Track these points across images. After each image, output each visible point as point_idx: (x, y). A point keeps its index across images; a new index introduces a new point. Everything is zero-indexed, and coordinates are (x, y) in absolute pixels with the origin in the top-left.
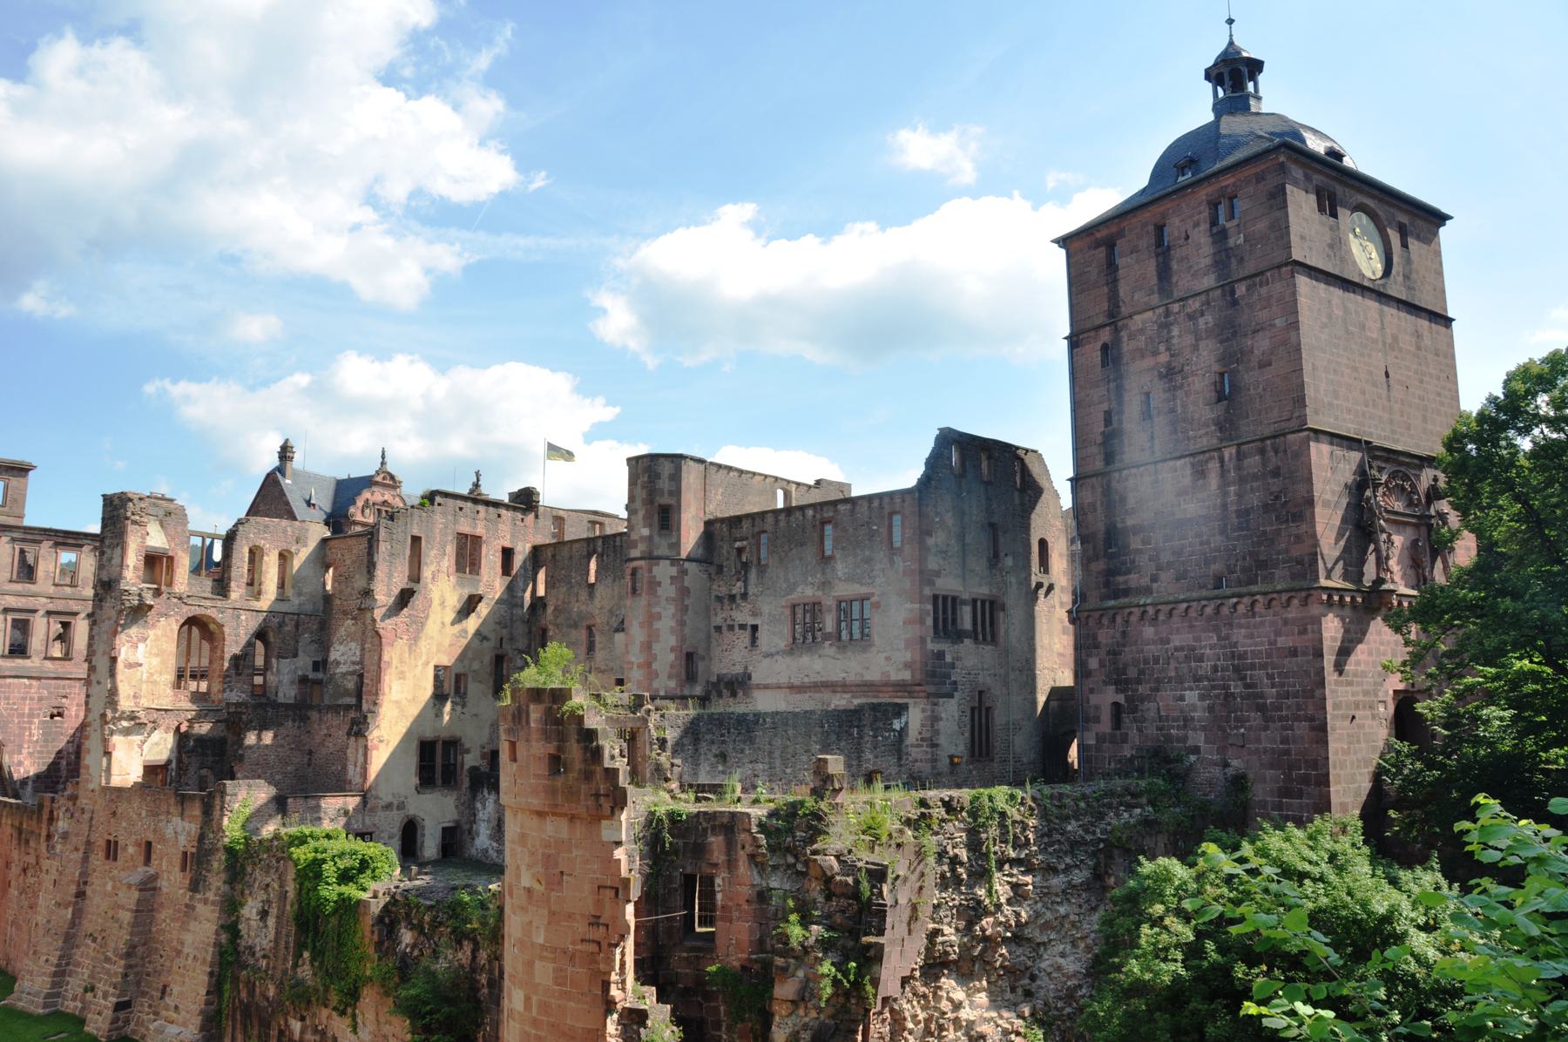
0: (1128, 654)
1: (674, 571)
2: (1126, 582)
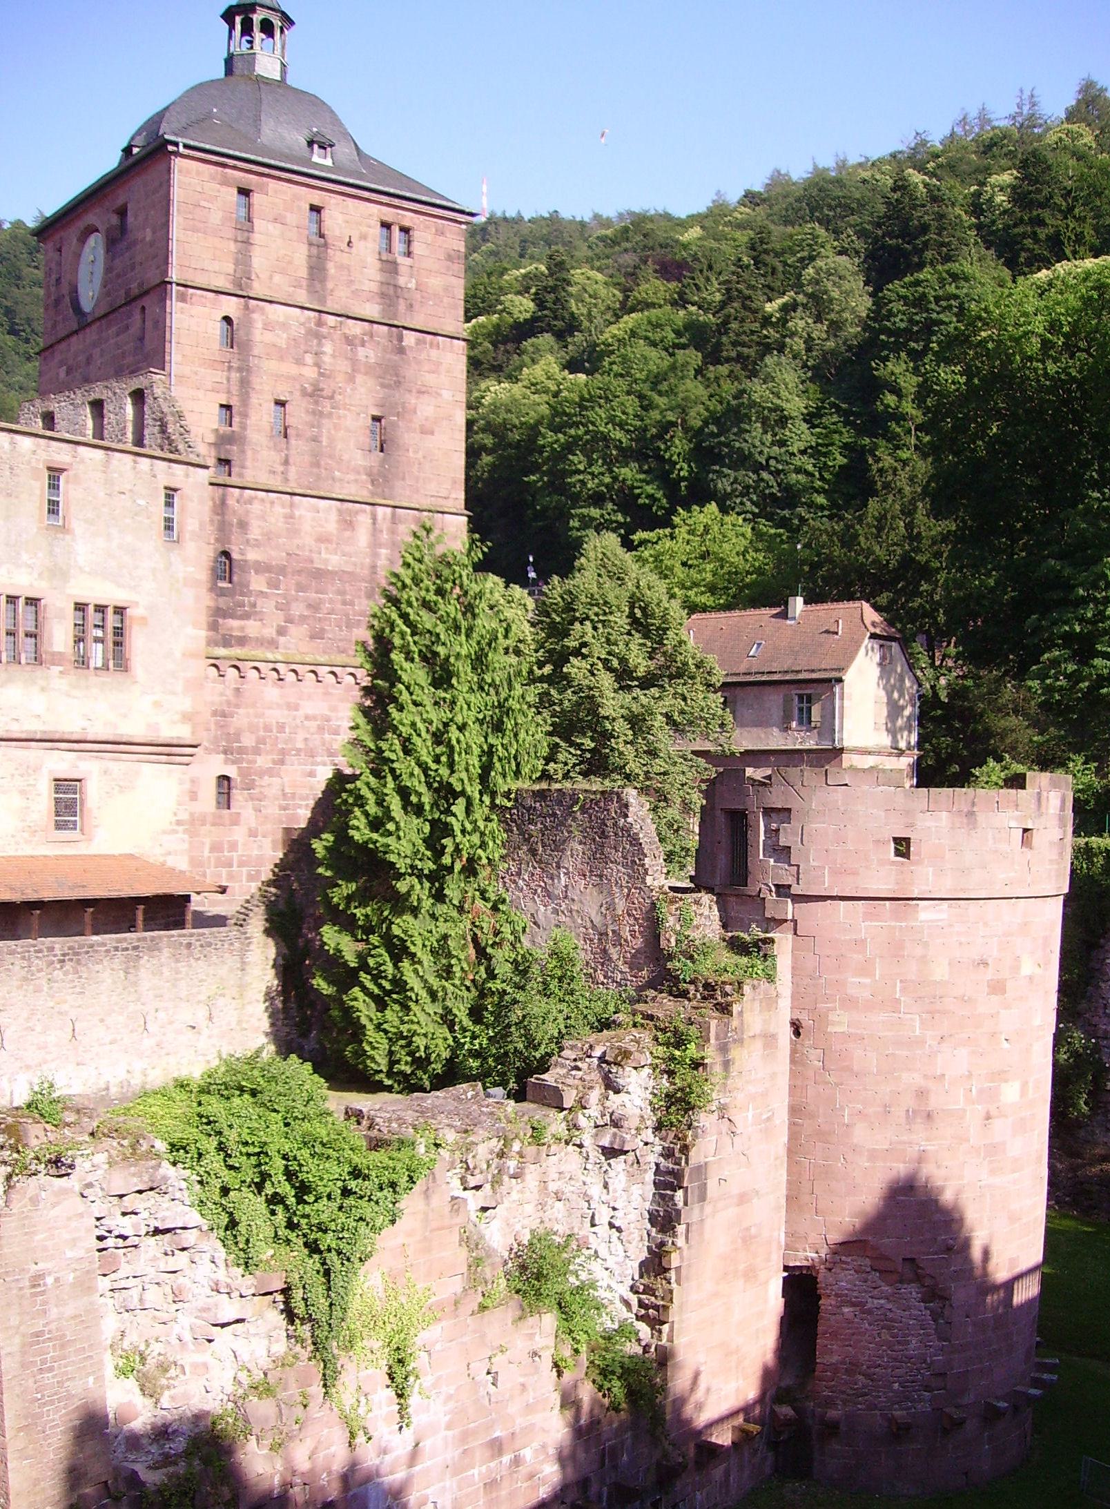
0: (241, 719)
2: (242, 629)
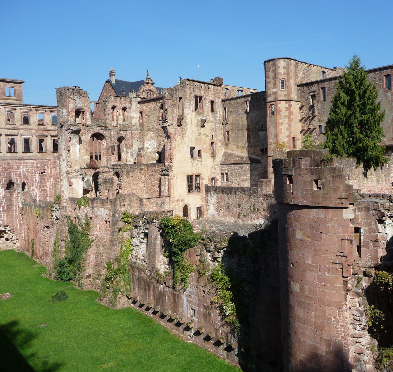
1: (287, 105)
